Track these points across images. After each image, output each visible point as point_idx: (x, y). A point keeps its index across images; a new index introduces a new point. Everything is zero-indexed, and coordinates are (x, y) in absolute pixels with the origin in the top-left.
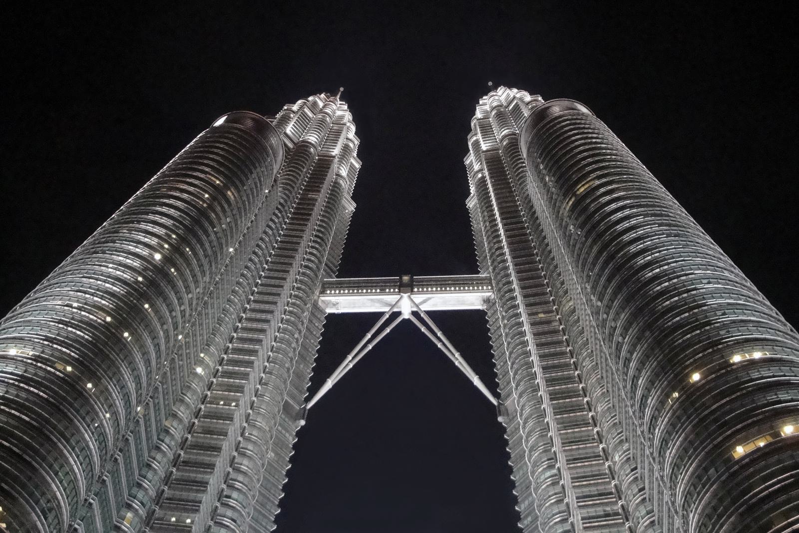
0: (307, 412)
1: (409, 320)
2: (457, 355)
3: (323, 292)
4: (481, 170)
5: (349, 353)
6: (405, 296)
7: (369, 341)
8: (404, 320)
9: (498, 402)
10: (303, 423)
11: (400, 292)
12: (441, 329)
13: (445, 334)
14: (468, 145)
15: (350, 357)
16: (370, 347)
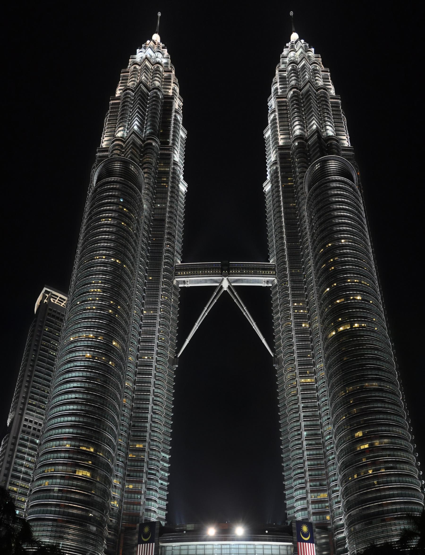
0: (178, 359)
1: (226, 290)
2: (254, 324)
3: (176, 275)
4: (275, 163)
5: (196, 322)
6: (225, 279)
7: (206, 311)
8: (224, 290)
9: (274, 355)
10: (177, 366)
11: (222, 275)
12: (245, 306)
13: (247, 308)
14: (268, 121)
15: (197, 324)
16: (206, 314)
